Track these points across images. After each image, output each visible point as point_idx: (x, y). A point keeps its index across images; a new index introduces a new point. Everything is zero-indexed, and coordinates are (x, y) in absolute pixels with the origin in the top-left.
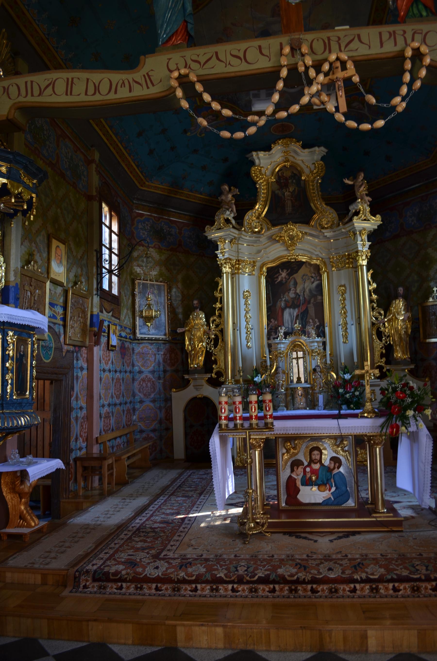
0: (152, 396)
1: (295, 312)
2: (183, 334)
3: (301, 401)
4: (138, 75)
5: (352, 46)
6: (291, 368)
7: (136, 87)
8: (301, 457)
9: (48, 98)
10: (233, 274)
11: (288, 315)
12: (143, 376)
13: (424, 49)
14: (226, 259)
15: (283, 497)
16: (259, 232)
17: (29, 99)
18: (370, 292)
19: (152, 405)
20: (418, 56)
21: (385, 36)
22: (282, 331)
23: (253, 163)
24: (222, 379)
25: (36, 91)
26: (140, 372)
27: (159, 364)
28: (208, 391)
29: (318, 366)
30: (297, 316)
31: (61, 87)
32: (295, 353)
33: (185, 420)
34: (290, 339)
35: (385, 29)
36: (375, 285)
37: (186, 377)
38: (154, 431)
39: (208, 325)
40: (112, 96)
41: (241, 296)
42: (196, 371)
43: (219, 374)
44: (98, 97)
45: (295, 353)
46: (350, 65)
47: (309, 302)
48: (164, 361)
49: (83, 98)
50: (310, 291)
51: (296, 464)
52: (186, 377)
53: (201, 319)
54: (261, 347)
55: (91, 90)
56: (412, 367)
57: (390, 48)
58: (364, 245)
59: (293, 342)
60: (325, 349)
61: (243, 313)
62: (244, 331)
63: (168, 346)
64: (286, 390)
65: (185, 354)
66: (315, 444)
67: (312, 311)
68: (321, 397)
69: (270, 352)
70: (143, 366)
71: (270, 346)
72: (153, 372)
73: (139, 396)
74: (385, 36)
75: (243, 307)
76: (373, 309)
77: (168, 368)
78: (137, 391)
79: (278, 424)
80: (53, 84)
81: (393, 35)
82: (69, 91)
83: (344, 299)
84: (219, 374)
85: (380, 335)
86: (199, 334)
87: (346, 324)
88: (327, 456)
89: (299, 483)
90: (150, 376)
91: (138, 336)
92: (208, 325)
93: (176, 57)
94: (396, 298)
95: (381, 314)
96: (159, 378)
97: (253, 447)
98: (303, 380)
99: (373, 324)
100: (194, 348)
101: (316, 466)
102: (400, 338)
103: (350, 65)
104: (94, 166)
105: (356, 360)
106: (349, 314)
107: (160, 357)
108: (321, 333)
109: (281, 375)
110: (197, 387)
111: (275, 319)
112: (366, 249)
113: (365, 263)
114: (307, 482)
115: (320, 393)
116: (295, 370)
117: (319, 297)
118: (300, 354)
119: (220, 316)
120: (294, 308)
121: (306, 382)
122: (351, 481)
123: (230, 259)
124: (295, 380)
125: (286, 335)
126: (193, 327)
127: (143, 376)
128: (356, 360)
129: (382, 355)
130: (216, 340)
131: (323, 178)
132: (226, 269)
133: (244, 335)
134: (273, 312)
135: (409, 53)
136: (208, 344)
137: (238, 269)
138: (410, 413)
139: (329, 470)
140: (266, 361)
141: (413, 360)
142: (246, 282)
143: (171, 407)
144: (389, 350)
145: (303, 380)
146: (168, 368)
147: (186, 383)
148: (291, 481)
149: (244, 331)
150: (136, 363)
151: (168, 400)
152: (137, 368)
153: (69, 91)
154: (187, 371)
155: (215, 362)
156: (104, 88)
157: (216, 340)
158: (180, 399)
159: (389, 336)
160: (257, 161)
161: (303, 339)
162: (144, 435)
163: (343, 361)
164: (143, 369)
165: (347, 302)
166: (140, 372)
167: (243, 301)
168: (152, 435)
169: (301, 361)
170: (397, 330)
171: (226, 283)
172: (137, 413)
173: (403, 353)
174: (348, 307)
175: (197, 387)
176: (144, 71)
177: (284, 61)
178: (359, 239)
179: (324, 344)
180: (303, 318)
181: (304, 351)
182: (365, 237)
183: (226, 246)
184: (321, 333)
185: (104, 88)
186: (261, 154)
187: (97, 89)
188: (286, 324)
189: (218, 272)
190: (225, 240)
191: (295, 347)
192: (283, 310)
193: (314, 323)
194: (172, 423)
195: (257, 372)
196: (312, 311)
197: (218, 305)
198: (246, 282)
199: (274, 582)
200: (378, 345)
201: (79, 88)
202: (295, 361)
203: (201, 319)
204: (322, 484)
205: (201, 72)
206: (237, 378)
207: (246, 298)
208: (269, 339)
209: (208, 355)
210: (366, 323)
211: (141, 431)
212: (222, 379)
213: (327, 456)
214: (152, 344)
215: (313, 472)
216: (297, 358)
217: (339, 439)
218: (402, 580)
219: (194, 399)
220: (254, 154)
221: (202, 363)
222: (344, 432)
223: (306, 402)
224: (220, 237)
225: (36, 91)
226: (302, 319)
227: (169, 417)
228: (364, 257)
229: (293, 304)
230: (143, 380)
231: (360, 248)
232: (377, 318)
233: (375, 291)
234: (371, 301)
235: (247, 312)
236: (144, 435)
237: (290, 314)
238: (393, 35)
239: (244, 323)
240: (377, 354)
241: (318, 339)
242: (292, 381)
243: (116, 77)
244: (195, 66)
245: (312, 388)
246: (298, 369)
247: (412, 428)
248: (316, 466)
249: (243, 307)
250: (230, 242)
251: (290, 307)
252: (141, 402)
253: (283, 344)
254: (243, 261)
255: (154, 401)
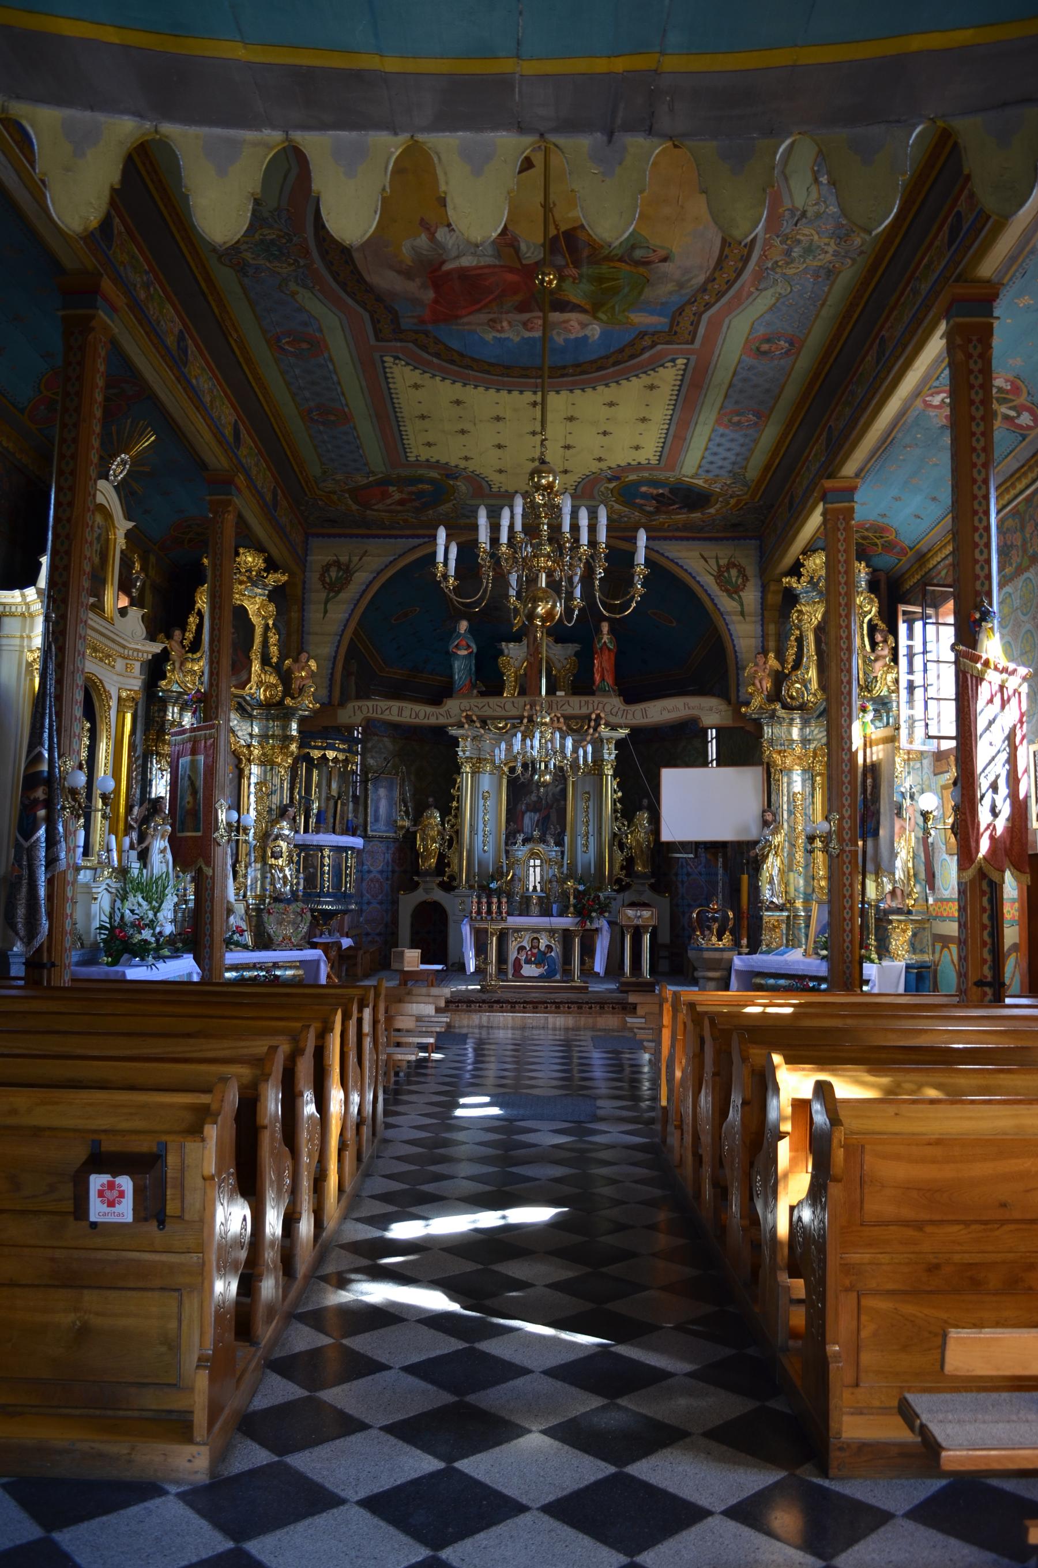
0: (380, 897)
1: (536, 817)
2: (415, 833)
3: (534, 909)
4: (442, 710)
5: (564, 707)
6: (528, 876)
7: (441, 717)
8: (525, 944)
9: (386, 716)
10: (473, 773)
11: (529, 820)
12: (372, 875)
13: (602, 715)
14: (467, 758)
15: (510, 972)
16: (503, 728)
17: (374, 715)
18: (614, 802)
19: (379, 906)
20: (598, 716)
21: (583, 703)
22: (520, 838)
23: (501, 653)
24: (455, 884)
25: (379, 711)
26: (369, 872)
27: (388, 863)
28: (438, 895)
29: (555, 875)
30: (538, 821)
31: (395, 711)
32: (532, 861)
33: (412, 925)
34: (529, 846)
35: (584, 699)
36: (620, 794)
37: (416, 878)
38: (379, 934)
39: (443, 825)
40: (426, 721)
41: (481, 797)
42: (427, 873)
43: (452, 878)
44: (417, 720)
45: (532, 861)
46: (562, 720)
47: (551, 808)
48: (393, 861)
49: (408, 720)
50: (553, 794)
51: (521, 948)
52: (416, 878)
53: (435, 817)
54: (498, 851)
55: (413, 716)
56: (653, 881)
57: (584, 711)
58: (610, 754)
59: (531, 850)
60: (562, 858)
61: (481, 814)
62: (481, 833)
63: (397, 845)
64: (522, 897)
65: (417, 854)
66: (535, 935)
67: (554, 817)
68: (555, 906)
69: (507, 857)
70: (372, 865)
71: (507, 852)
72: (381, 872)
73: (367, 897)
74: (583, 703)
75: (481, 808)
76: (617, 819)
77: (397, 869)
78: (365, 892)
79: (510, 919)
80: (390, 708)
81: (587, 703)
82: (400, 714)
83: (588, 807)
84: (452, 878)
85: (621, 846)
86: (432, 833)
87: (587, 833)
88: (543, 943)
89: (522, 962)
90: (379, 876)
91: (369, 833)
92: (443, 825)
93: (465, 703)
94: (640, 810)
95: (624, 825)
96: (387, 879)
97: (492, 934)
98: (538, 889)
99: (615, 835)
100: (426, 849)
101: (535, 951)
102: (642, 851)
103: (562, 720)
104: (353, 678)
105: (592, 871)
106: (591, 823)
107: (389, 857)
108: (560, 843)
109: (516, 882)
110: (427, 891)
111: (515, 823)
112: (613, 756)
113: (611, 772)
114: (528, 962)
115: (555, 902)
116: (532, 878)
117: (563, 803)
118: (538, 862)
119: (456, 816)
120: (535, 812)
121: (542, 891)
122: (559, 962)
123: (472, 758)
124: (531, 888)
125: (525, 841)
126: (427, 826)
127: (372, 875)
128: (592, 871)
129: (622, 868)
130: (451, 841)
131: (574, 675)
132: (468, 769)
133: (481, 838)
134: (513, 816)
135: (593, 716)
136: (441, 845)
137: (479, 768)
138: (594, 914)
139: (544, 954)
140: (502, 867)
141: (653, 874)
142: (486, 782)
143: (397, 911)
144: (630, 862)
145: (538, 889)
146: (397, 869)
147: (416, 885)
148: (517, 960)
149: (481, 833)
150: (365, 862)
151: (395, 902)
152: (365, 867)
153: (400, 714)
154: (418, 873)
155: (448, 865)
156: (422, 715)
157: (451, 841)
158: (408, 902)
159: (631, 848)
160: (506, 651)
161: (541, 848)
162: (370, 938)
163: (580, 872)
164: (372, 868)
165: (591, 810)
166: (369, 872)
167: (481, 802)
168: (377, 938)
169: (538, 870)
170: (638, 841)
171: (466, 780)
172: (364, 914)
173: (644, 867)
174: (591, 816)
175: (427, 891)
176: (445, 709)
177: (526, 714)
178: (606, 747)
179: (563, 853)
180: (544, 824)
181: (541, 859)
182: (612, 746)
183: (468, 744)
184: (560, 843)
185: (422, 715)
186: (511, 645)
187: (417, 716)
188: (525, 830)
189: (457, 769)
190: (467, 737)
191: (534, 855)
192: (523, 813)
193: (556, 829)
194: (397, 927)
195: (493, 878)
196: (554, 817)
197: (455, 804)
198: (486, 782)
199: (503, 1002)
200: (619, 857)
201: (406, 713)
202: (532, 869)
203: (435, 817)
204: (538, 964)
205: (479, 713)
206: (471, 883)
207: (485, 798)
208: (506, 844)
209: (441, 857)
210: (606, 837)
211: (368, 934)
212: (455, 884)
213: (543, 943)
214: (381, 842)
215: (533, 955)
216: (535, 866)
217: (552, 932)
218: (572, 1003)
219: (425, 902)
220: (504, 644)
221: (434, 865)
222: (554, 926)
223: (540, 910)
224: (463, 735)
225: (379, 711)
226: (543, 824)
227: (395, 922)
228: (609, 766)
229: (534, 808)
230: (372, 880)
231: (606, 756)
232: (619, 829)
233: (620, 800)
234: (615, 811)
235: (485, 814)
236: (370, 938)
237: (531, 819)
238: (587, 703)
239: (481, 826)
240: (617, 866)
241: (557, 849)
242: (528, 889)
243: (429, 709)
244: (475, 709)
245: (548, 897)
246: (535, 877)
247: (595, 926)
248: (535, 951)
249: (481, 808)
250: (472, 740)
251: (531, 811)
252: (369, 903)
253: (521, 851)
254: (485, 759)
255: (381, 903)
